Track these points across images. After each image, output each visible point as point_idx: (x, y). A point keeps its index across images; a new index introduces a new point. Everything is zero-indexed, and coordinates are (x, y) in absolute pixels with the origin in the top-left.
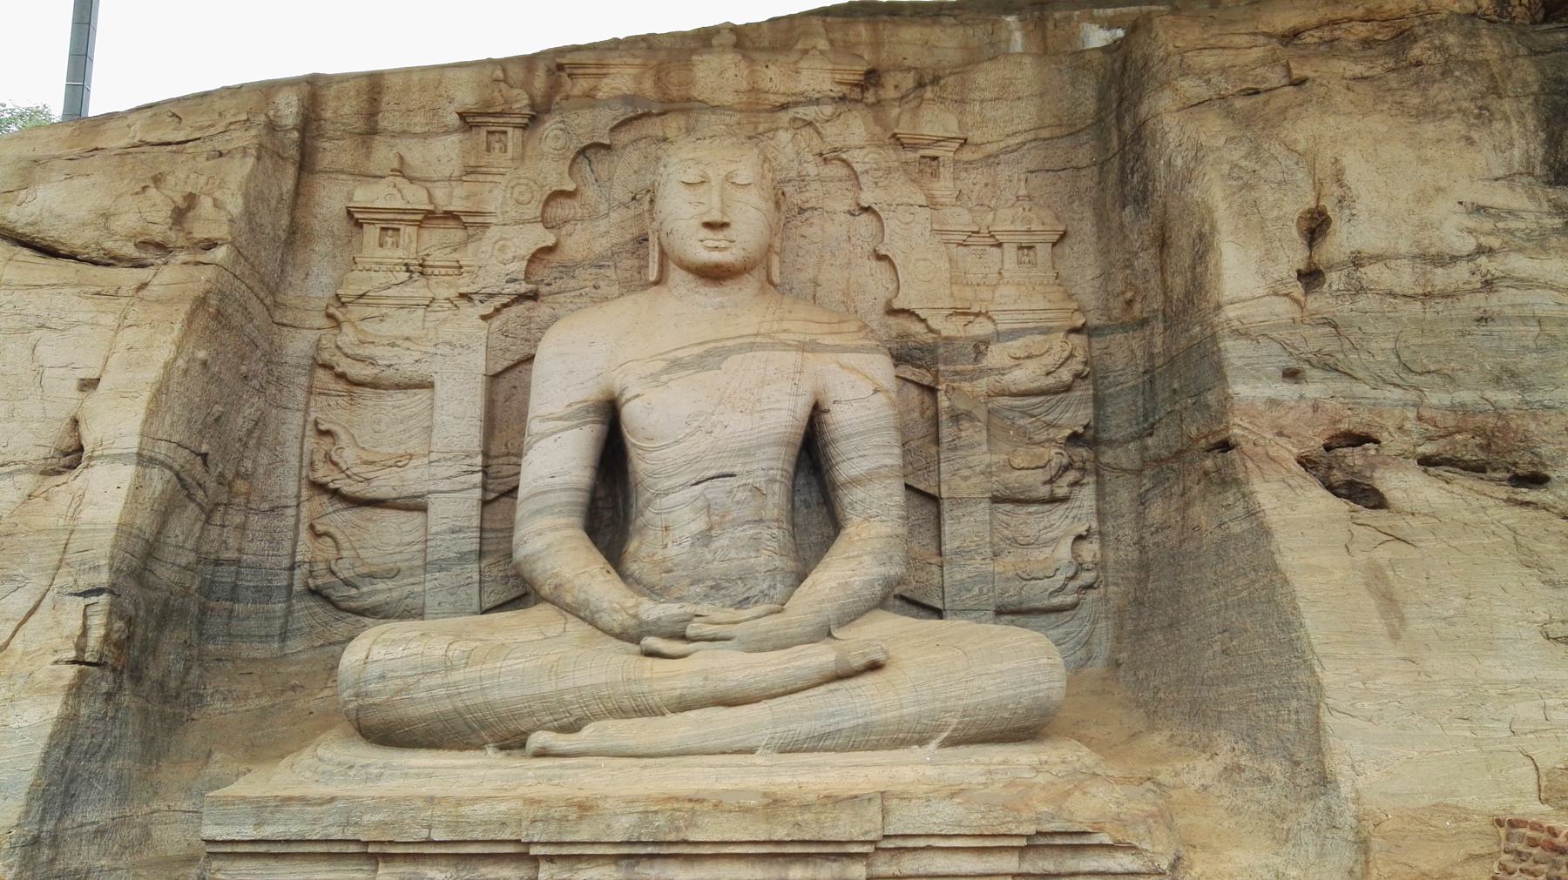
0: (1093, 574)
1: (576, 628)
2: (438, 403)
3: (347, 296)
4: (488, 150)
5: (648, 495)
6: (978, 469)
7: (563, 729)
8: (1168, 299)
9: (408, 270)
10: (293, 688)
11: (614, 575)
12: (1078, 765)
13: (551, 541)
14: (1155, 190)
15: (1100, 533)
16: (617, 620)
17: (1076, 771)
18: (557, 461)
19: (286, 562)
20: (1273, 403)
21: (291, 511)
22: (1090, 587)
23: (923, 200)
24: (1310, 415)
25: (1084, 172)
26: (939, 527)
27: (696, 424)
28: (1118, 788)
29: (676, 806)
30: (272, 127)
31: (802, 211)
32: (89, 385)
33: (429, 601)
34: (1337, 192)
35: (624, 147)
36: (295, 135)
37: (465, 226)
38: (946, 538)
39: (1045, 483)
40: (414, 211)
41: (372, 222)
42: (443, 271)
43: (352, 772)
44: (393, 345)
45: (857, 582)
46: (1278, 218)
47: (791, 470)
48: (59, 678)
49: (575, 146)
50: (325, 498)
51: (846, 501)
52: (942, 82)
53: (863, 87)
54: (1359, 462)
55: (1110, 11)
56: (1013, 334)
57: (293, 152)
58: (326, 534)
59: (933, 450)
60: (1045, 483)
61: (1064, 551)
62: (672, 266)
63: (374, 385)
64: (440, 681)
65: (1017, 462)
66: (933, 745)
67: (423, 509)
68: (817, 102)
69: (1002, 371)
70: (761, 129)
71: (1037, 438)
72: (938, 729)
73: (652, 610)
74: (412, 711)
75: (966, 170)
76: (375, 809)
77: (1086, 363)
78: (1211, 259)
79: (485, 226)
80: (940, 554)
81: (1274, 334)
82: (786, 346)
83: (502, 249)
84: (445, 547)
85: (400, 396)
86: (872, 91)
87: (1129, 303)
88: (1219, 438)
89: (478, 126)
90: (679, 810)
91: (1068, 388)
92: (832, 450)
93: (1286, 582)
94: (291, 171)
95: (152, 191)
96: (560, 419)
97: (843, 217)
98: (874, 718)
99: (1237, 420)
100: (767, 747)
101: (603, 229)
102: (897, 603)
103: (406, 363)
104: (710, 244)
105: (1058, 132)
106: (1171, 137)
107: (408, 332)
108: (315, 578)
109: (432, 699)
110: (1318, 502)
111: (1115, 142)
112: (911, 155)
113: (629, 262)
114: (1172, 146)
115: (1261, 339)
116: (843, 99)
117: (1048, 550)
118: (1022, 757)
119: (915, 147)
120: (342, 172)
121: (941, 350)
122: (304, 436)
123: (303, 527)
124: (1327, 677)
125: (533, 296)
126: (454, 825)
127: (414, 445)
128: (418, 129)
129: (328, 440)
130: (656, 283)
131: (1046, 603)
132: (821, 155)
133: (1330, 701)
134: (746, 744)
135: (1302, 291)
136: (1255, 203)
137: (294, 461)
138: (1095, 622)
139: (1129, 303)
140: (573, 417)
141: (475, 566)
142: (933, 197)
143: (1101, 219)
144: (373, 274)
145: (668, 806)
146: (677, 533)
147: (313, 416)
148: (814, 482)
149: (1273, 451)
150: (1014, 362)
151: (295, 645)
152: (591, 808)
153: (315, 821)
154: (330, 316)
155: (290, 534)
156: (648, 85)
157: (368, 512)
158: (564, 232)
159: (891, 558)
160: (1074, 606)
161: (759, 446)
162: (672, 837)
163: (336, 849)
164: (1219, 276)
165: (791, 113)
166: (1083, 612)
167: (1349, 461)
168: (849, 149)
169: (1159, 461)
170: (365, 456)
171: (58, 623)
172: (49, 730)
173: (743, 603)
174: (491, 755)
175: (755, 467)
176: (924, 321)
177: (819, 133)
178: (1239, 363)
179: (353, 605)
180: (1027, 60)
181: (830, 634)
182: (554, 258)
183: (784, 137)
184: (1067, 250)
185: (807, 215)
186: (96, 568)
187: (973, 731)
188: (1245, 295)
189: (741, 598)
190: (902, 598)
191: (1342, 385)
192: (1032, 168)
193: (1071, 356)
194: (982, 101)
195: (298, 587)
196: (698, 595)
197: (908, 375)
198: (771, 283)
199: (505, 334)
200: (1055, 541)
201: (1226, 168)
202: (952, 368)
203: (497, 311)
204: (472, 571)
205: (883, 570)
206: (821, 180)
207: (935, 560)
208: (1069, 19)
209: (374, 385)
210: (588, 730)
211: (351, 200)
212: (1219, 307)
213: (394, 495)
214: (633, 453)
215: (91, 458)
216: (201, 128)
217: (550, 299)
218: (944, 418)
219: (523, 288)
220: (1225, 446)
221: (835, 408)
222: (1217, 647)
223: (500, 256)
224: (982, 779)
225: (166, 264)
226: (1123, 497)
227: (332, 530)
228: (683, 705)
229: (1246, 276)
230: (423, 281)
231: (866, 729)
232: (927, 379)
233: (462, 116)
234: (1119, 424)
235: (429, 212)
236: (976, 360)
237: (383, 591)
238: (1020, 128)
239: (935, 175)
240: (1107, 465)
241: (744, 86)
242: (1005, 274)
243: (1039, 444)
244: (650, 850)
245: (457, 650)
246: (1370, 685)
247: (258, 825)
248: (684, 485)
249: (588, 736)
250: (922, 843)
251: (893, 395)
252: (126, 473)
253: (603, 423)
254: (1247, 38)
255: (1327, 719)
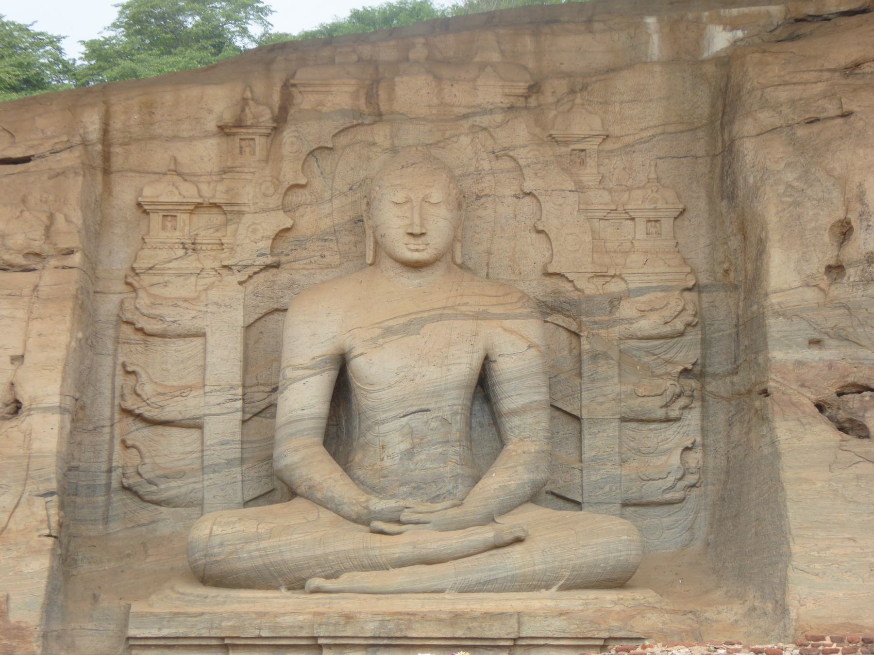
0: (696, 477)
1: (327, 515)
2: (209, 349)
3: (140, 268)
4: (241, 153)
5: (369, 422)
6: (611, 397)
7: (328, 577)
8: (746, 276)
9: (184, 248)
10: (128, 556)
11: (349, 480)
12: (642, 602)
13: (302, 454)
14: (737, 196)
15: (703, 445)
16: (354, 510)
17: (640, 605)
18: (305, 398)
19: (104, 467)
20: (799, 363)
21: (107, 430)
22: (694, 486)
23: (572, 186)
24: (826, 372)
25: (700, 161)
26: (580, 440)
27: (402, 374)
28: (666, 615)
29: (400, 617)
30: (85, 143)
31: (479, 197)
32: (18, 359)
33: (206, 495)
34: (859, 207)
35: (344, 148)
36: (99, 147)
37: (225, 213)
38: (585, 449)
39: (662, 407)
40: (188, 204)
41: (156, 211)
42: (209, 247)
43: (208, 600)
44: (176, 306)
45: (512, 484)
46: (815, 228)
47: (469, 404)
48: (45, 545)
49: (306, 149)
50: (130, 420)
51: (508, 426)
52: (589, 88)
53: (526, 98)
54: (857, 405)
55: (735, 11)
56: (640, 292)
57: (98, 161)
58: (133, 447)
59: (577, 381)
60: (662, 407)
61: (675, 459)
62: (383, 254)
63: (163, 335)
64: (255, 548)
65: (641, 391)
66: (554, 589)
67: (200, 427)
68: (491, 112)
69: (630, 321)
70: (448, 134)
71: (659, 372)
72: (557, 579)
73: (379, 504)
74: (239, 565)
75: (608, 158)
76: (229, 619)
77: (695, 316)
78: (764, 256)
79: (241, 213)
80: (581, 461)
81: (804, 315)
82: (465, 316)
83: (254, 231)
84: (214, 456)
85: (181, 342)
86: (534, 97)
87: (727, 271)
88: (762, 388)
89: (234, 134)
90: (402, 619)
91: (682, 334)
92: (498, 389)
93: (783, 489)
94: (100, 177)
95: (26, 214)
96: (307, 368)
97: (510, 200)
98: (517, 572)
99: (773, 376)
100: (451, 589)
101: (327, 211)
102: (549, 497)
103: (186, 319)
104: (412, 247)
105: (680, 127)
106: (749, 159)
107: (184, 293)
108: (127, 478)
109: (252, 558)
110: (824, 433)
111: (720, 144)
112: (563, 150)
113: (347, 238)
114: (748, 166)
115: (794, 318)
116: (511, 108)
117: (664, 458)
118: (608, 596)
119: (566, 143)
120: (131, 171)
121: (584, 306)
122: (114, 375)
123: (117, 442)
124: (796, 549)
125: (276, 266)
126: (273, 628)
127: (192, 379)
128: (185, 135)
129: (132, 377)
130: (371, 265)
131: (660, 498)
132: (494, 153)
133: (794, 563)
134: (439, 587)
135: (827, 282)
136: (799, 217)
137: (108, 393)
138: (697, 513)
139: (727, 271)
140: (315, 367)
141: (239, 469)
142: (581, 182)
143: (711, 201)
144: (159, 252)
145: (396, 617)
146: (390, 451)
147: (121, 360)
148: (486, 409)
149: (794, 399)
150: (640, 314)
151: (115, 527)
152: (352, 618)
153: (193, 627)
154: (128, 284)
155: (106, 446)
156: (362, 103)
157: (160, 429)
158: (297, 214)
159: (537, 467)
160: (682, 500)
161: (446, 390)
162: (398, 635)
163: (204, 642)
164: (768, 272)
165: (471, 121)
166: (689, 505)
167: (850, 404)
168: (515, 148)
169: (740, 394)
170: (160, 390)
171: (33, 513)
172: (46, 574)
173: (434, 499)
174: (284, 592)
175: (443, 404)
176: (572, 281)
177: (492, 136)
178: (777, 336)
179: (154, 498)
180: (657, 68)
181: (493, 520)
182: (291, 235)
183: (465, 140)
184: (686, 223)
185: (483, 200)
186: (49, 480)
187: (579, 581)
188: (785, 286)
189: (433, 495)
190: (553, 494)
191: (851, 351)
192: (661, 155)
193: (684, 309)
194: (621, 103)
195: (115, 484)
196: (405, 493)
197: (560, 322)
198: (455, 263)
199: (256, 295)
200: (668, 452)
201: (781, 189)
202: (592, 319)
203: (250, 277)
204: (236, 472)
205: (531, 476)
206: (492, 172)
207: (577, 465)
208: (697, 21)
209: (163, 335)
210: (344, 577)
211: (141, 195)
212: (766, 295)
213: (180, 417)
214: (357, 391)
215: (30, 410)
216: (32, 147)
217: (287, 266)
218: (585, 357)
219: (269, 260)
220: (765, 393)
221: (500, 360)
222: (753, 531)
223: (252, 238)
224: (581, 608)
225: (43, 269)
226: (721, 418)
227: (137, 444)
228: (401, 563)
229: (786, 273)
230: (194, 257)
231: (513, 578)
232: (574, 327)
233: (221, 128)
234: (719, 363)
235: (199, 204)
236: (610, 312)
237: (174, 488)
238: (651, 124)
239: (583, 163)
240: (711, 393)
241: (435, 101)
242: (636, 243)
243: (659, 376)
244: (385, 642)
245: (263, 529)
246: (822, 554)
247: (160, 629)
248: (395, 418)
249: (344, 581)
250: (542, 642)
251: (543, 349)
252: (55, 419)
253: (335, 369)
254: (815, 74)
255: (791, 574)
